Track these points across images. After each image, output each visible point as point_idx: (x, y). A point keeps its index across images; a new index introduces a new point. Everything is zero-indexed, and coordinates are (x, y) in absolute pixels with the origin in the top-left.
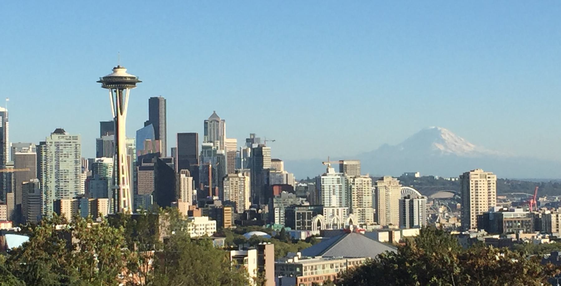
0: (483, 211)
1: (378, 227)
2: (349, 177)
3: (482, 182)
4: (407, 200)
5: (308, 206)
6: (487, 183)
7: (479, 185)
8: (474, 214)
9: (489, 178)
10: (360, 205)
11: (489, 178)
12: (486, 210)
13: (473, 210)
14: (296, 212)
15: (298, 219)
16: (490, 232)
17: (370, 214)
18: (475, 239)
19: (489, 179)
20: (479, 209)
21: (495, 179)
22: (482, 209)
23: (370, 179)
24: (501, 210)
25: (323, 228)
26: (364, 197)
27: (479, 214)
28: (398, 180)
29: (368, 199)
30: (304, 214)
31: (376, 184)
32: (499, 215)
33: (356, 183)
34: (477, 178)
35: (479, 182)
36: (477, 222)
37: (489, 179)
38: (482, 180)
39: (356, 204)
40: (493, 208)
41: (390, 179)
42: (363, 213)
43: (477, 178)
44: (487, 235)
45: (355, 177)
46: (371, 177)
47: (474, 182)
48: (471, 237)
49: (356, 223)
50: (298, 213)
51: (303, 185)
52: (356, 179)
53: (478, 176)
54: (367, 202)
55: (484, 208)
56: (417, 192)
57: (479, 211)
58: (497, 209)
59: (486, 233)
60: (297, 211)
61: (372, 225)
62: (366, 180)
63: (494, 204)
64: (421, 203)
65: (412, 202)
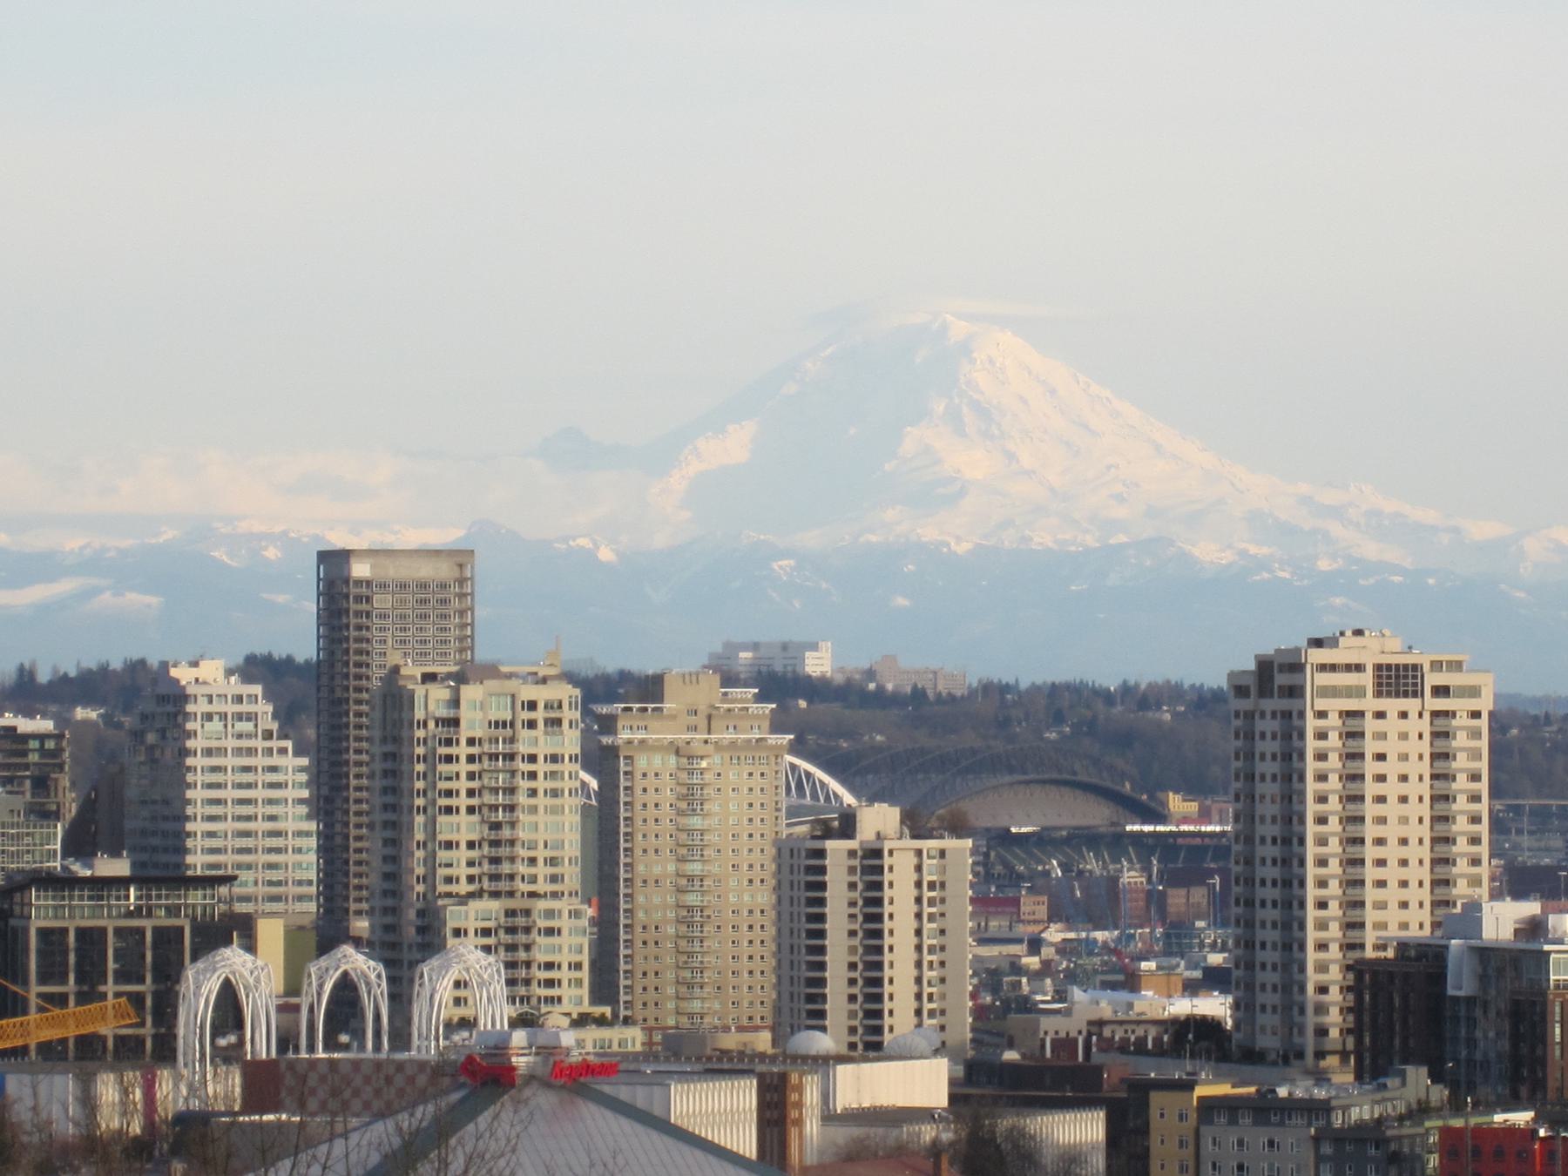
0: (1393, 931)
1: (633, 1038)
2: (417, 672)
3: (1392, 725)
4: (836, 848)
5: (123, 882)
6: (1425, 725)
7: (1370, 747)
8: (1334, 951)
9: (1441, 691)
10: (495, 877)
11: (1441, 691)
12: (1418, 924)
13: (1322, 925)
14: (36, 924)
15: (44, 979)
16: (1462, 1086)
17: (568, 943)
18: (1369, 1135)
19: (1442, 704)
20: (1370, 915)
21: (1485, 704)
22: (1393, 916)
23: (567, 692)
24: (1534, 928)
25: (261, 1044)
26: (523, 817)
27: (1370, 953)
28: (761, 698)
29: (554, 828)
30: (91, 939)
31: (609, 724)
32: (1520, 963)
33: (465, 714)
34: (1359, 692)
35: (1370, 725)
36: (1355, 1010)
37: (1442, 704)
38: (1392, 705)
39: (463, 871)
40: (1474, 907)
41: (709, 691)
42: (512, 940)
43: (1359, 692)
44: (1456, 1106)
45: (461, 678)
46: (570, 678)
47: (1334, 720)
48: (1337, 1121)
49: (494, 1010)
50: (44, 933)
51: (25, 725)
52: (470, 692)
53: (1367, 679)
54: (541, 854)
55: (1399, 915)
56: (834, 785)
57: (1370, 937)
58: (1501, 920)
59: (1439, 1094)
60: (41, 912)
61: (581, 1021)
62: (541, 694)
63: (1473, 876)
64: (923, 873)
65: (872, 861)
